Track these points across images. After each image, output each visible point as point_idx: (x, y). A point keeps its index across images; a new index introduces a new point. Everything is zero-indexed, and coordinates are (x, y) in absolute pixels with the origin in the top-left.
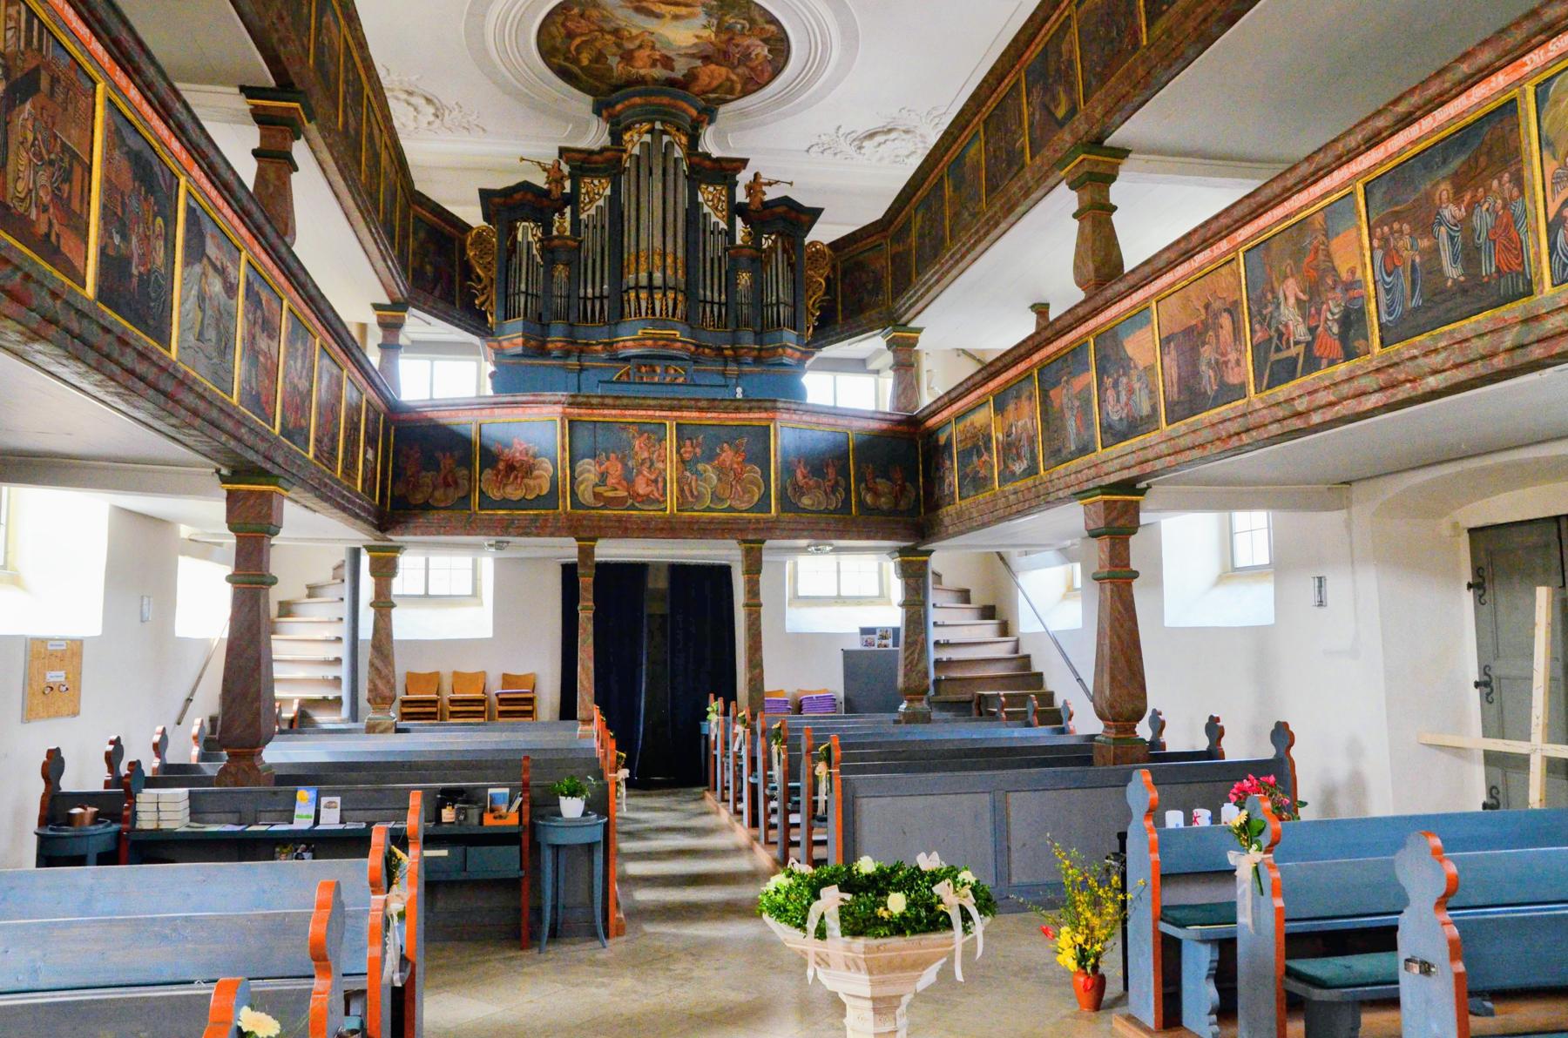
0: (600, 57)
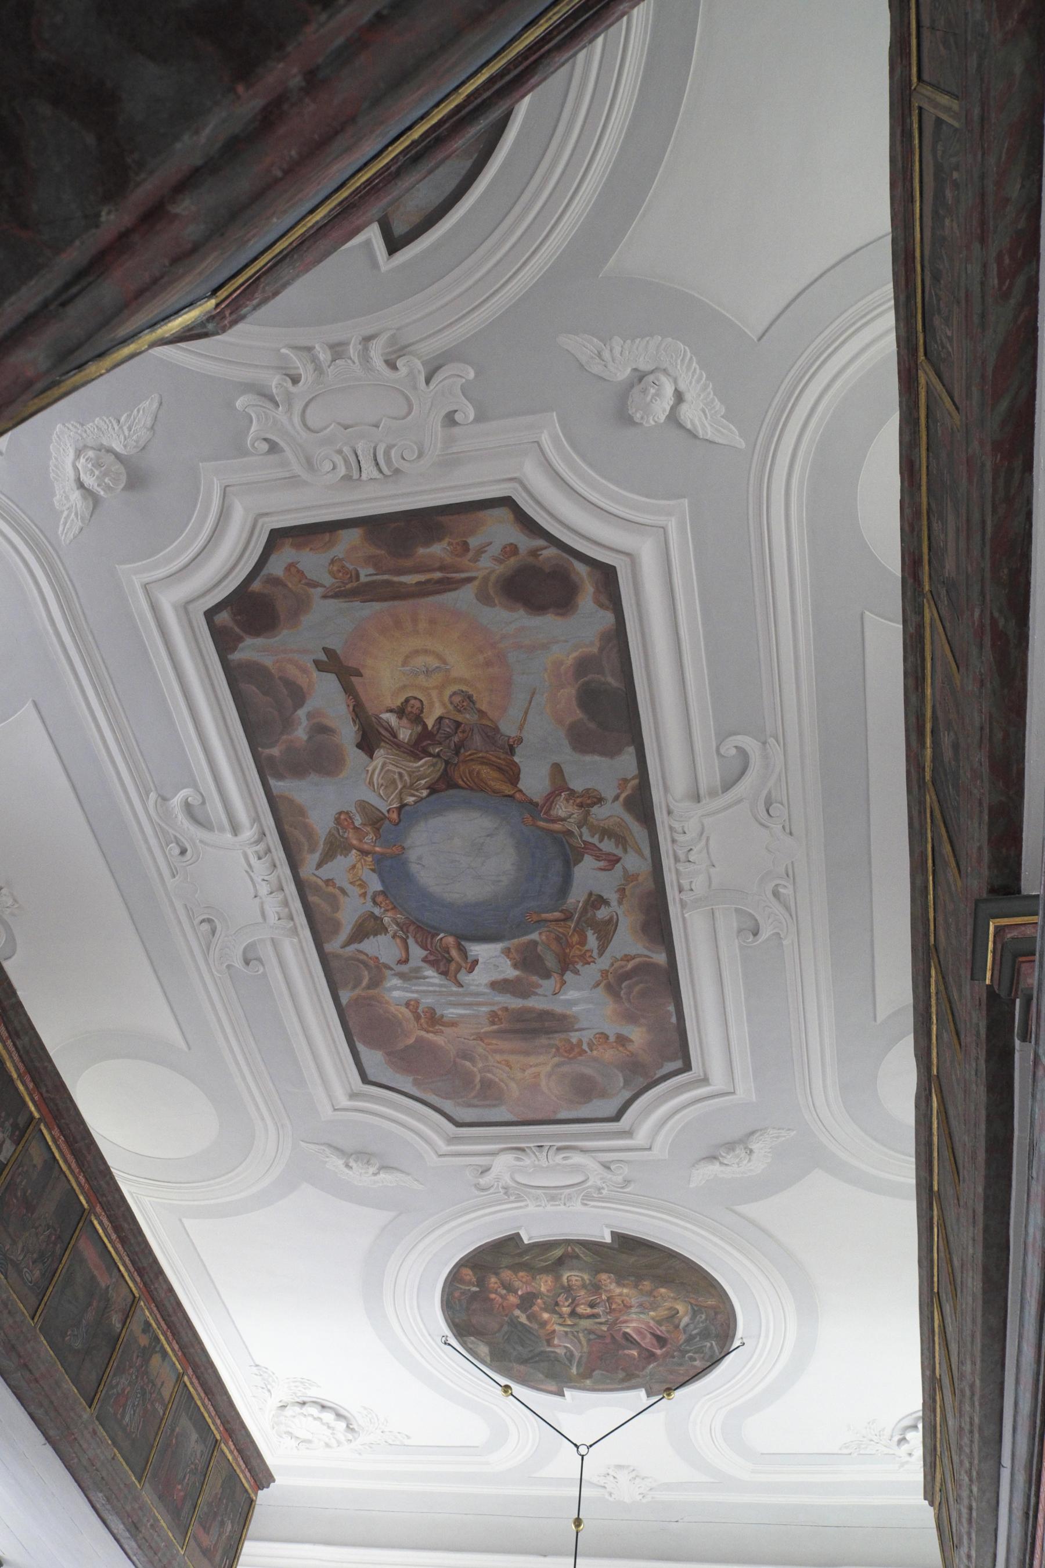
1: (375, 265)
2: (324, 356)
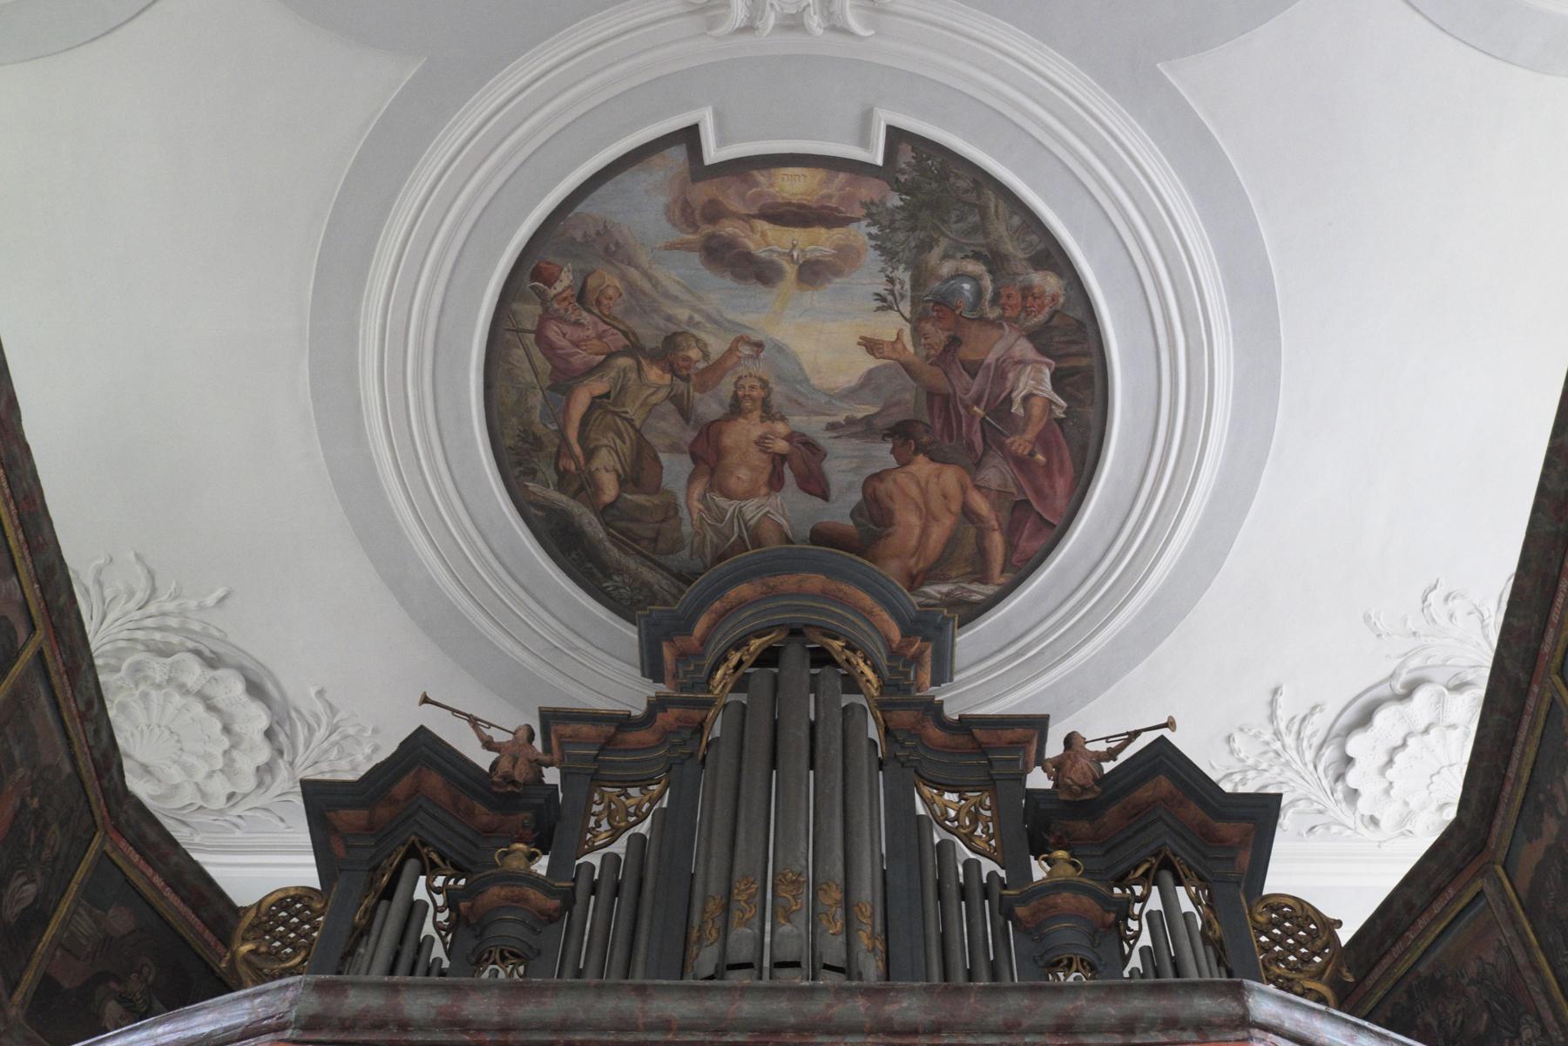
0: (640, 470)
1: (719, 116)
2: (815, 22)
